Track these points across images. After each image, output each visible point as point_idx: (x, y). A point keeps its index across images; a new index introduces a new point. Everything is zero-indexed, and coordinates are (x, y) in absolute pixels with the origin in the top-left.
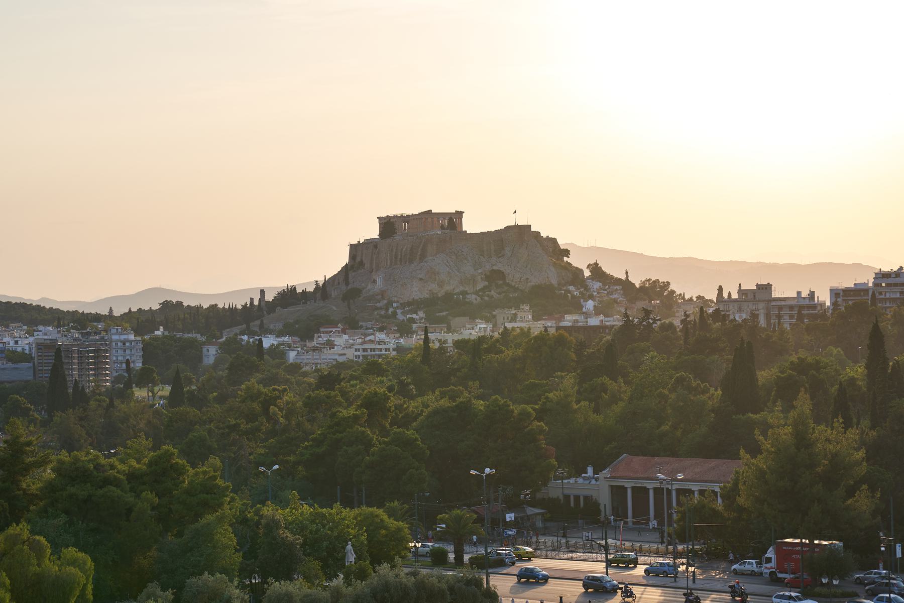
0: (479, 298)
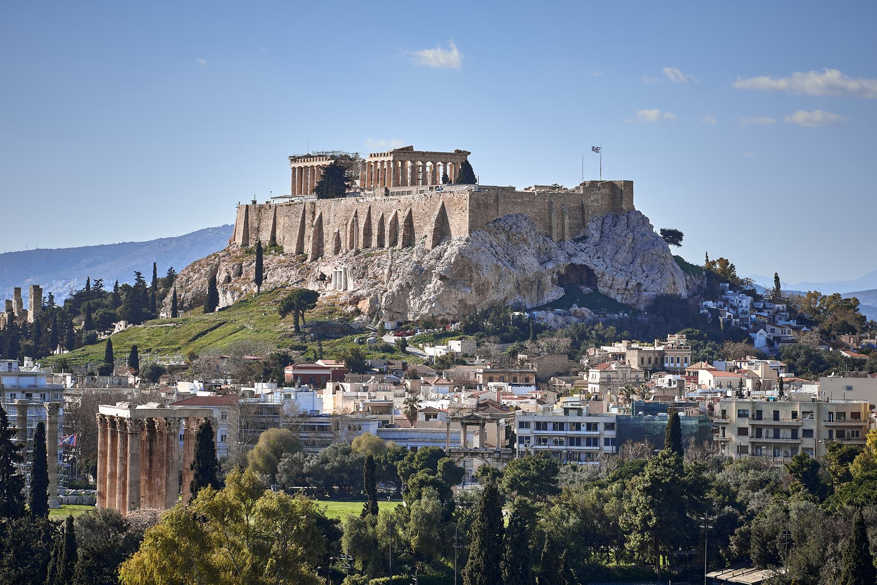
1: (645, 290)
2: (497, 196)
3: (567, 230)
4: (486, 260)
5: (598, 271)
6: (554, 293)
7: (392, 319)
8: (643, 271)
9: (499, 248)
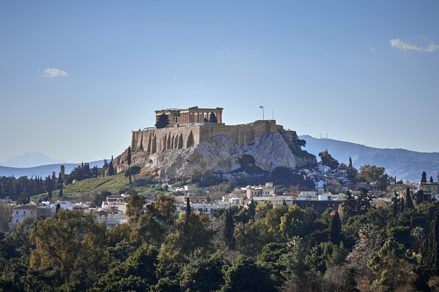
0: (233, 177)
1: (274, 165)
2: (212, 127)
4: (205, 153)
5: (255, 157)
6: (235, 167)
7: (169, 178)
8: (275, 157)
9: (212, 148)
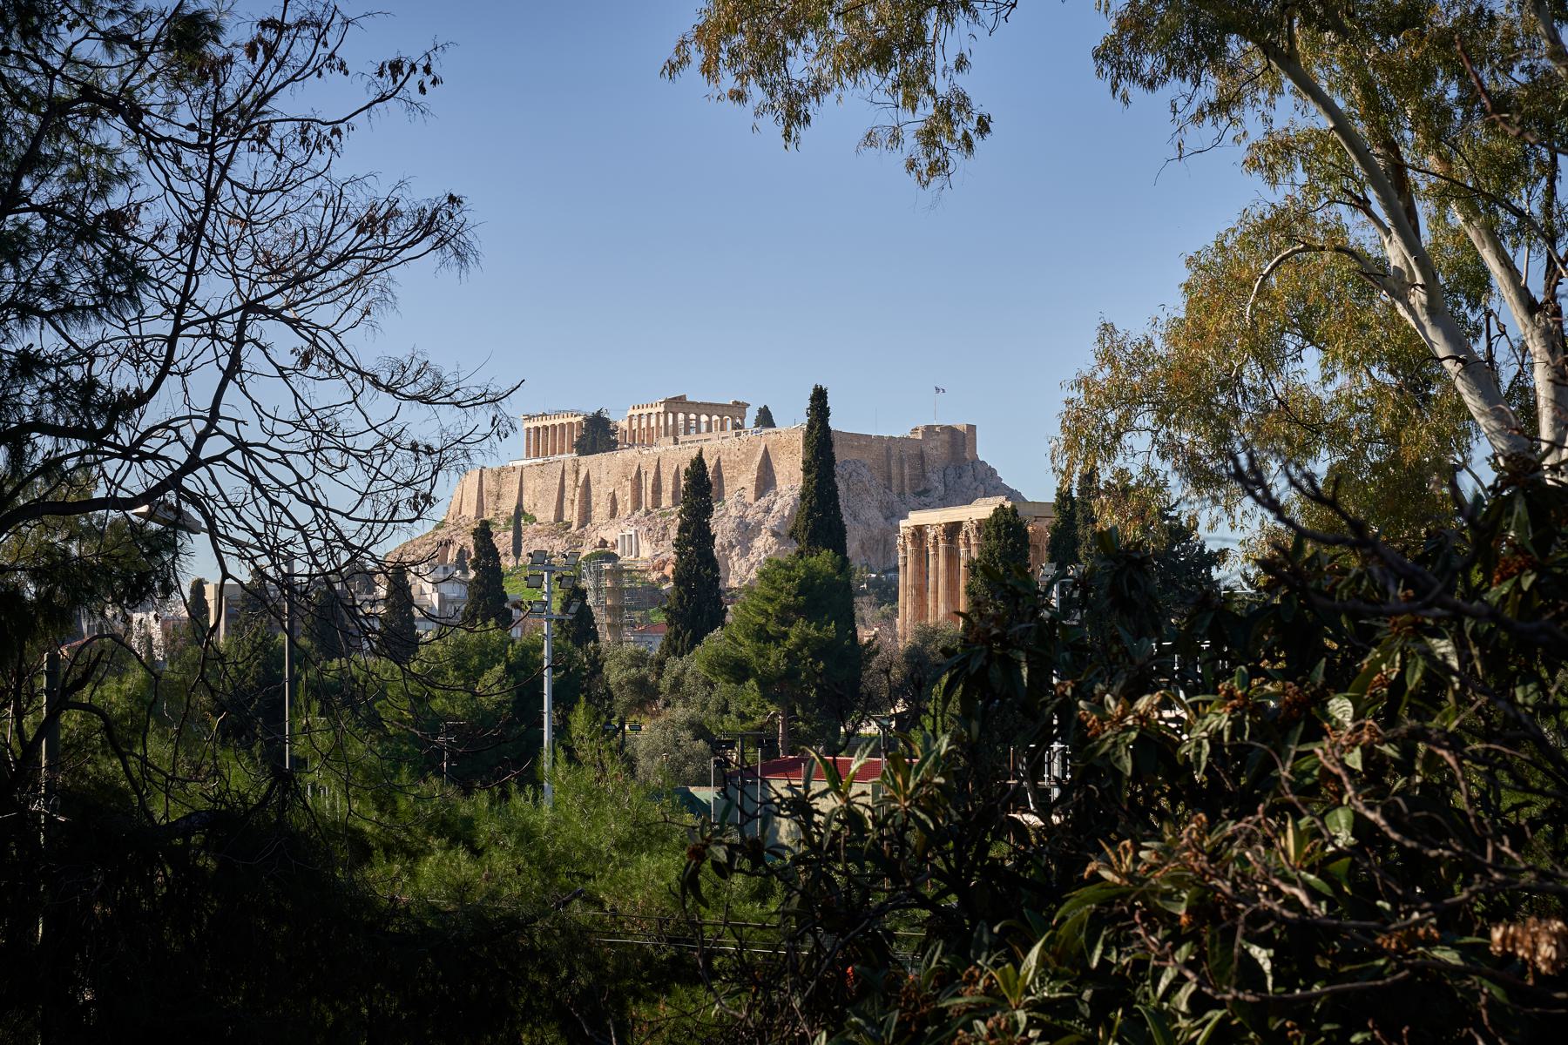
3: (907, 482)
